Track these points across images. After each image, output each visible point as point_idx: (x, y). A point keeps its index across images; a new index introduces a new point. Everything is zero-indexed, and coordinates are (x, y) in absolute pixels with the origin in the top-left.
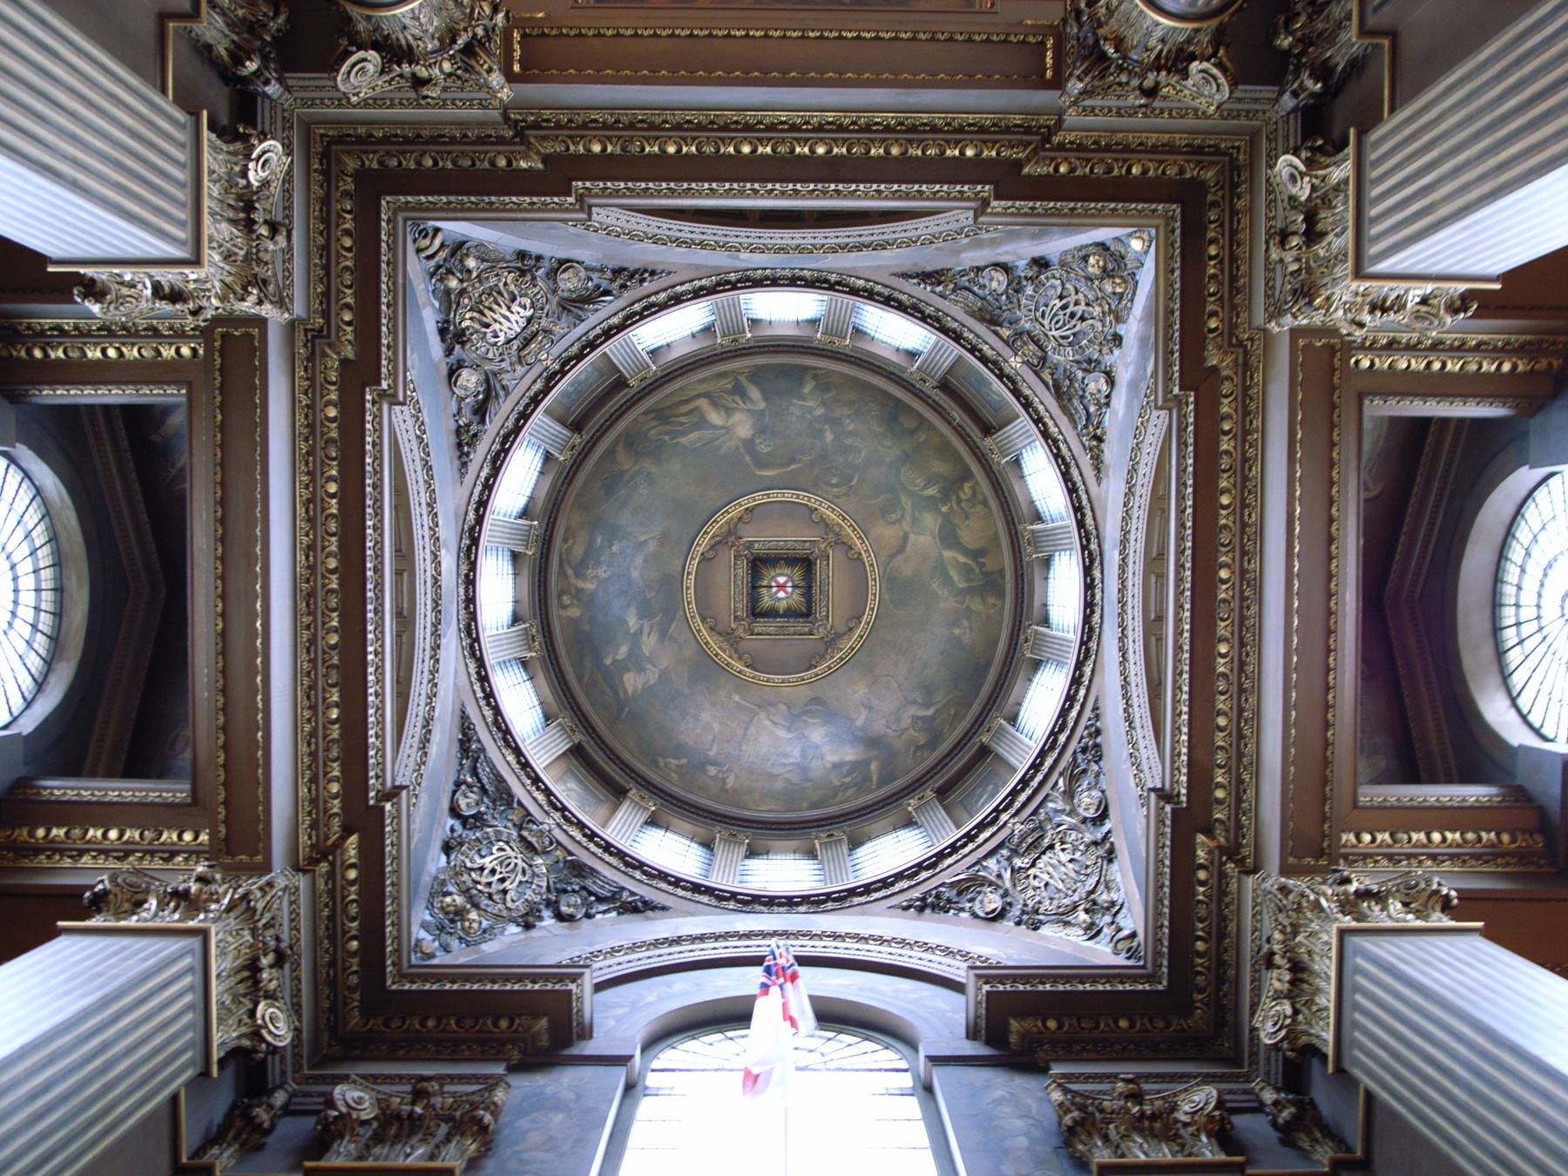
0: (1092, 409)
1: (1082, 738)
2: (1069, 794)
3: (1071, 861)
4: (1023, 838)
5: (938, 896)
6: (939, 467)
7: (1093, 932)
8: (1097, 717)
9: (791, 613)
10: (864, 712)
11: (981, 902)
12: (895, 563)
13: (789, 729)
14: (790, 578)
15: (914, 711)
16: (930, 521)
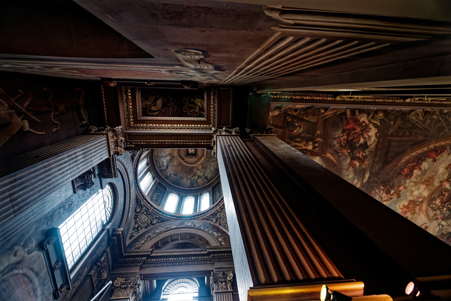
0: (211, 219)
1: (165, 218)
2: (156, 218)
3: (145, 221)
4: (149, 212)
5: (139, 201)
6: (209, 176)
7: (134, 229)
8: (168, 221)
9: (188, 152)
10: (172, 165)
11: (138, 208)
12: (195, 168)
13: (169, 154)
14: (193, 152)
15: (172, 172)
16: (202, 174)
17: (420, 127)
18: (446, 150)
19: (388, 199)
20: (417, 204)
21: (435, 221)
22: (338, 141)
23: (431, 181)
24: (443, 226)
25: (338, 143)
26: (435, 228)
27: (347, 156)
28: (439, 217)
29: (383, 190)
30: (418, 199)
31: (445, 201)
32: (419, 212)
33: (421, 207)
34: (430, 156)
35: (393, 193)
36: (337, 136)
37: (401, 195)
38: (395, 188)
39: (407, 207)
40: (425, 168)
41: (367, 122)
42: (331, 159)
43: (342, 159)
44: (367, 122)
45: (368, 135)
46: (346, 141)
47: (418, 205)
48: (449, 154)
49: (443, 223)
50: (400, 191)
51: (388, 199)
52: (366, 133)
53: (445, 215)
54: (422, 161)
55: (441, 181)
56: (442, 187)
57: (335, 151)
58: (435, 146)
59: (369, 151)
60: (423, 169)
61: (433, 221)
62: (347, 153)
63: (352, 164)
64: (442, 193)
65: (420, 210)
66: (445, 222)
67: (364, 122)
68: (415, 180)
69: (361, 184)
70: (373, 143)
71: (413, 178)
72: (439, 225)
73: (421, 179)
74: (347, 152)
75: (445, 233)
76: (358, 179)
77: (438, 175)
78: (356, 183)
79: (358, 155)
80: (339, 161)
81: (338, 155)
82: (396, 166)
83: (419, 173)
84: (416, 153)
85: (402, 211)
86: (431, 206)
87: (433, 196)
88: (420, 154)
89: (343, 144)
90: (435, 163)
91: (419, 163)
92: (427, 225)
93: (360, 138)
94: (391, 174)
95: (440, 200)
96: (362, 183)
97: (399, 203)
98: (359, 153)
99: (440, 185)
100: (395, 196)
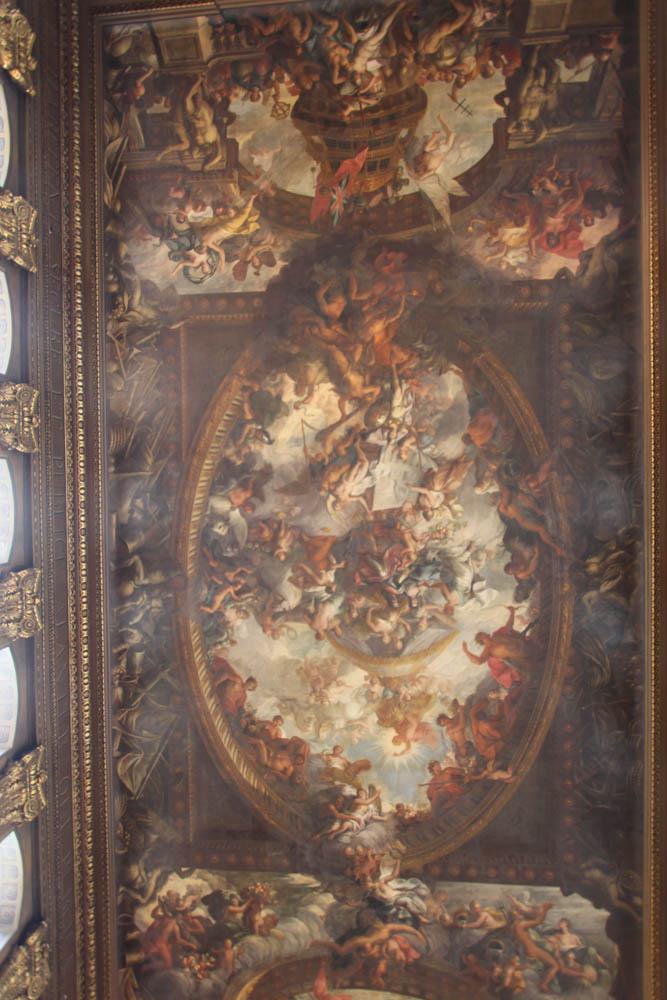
17: (160, 754)
18: (222, 656)
19: (373, 798)
20: (394, 697)
21: (455, 616)
22: (203, 975)
23: (314, 673)
24: (476, 579)
25: (209, 977)
26: (482, 603)
27: (243, 945)
28: (441, 602)
29: (343, 821)
30: (375, 697)
31: (385, 601)
32: (420, 683)
33: (401, 679)
34: (238, 701)
35: (354, 786)
36: (192, 981)
37: (362, 758)
38: (337, 783)
39: (401, 727)
40: (274, 705)
41: (153, 905)
42: (252, 989)
43: (250, 960)
44: (153, 905)
45: (185, 897)
46: (203, 956)
47: (397, 693)
48: (233, 643)
49: (464, 581)
50: (348, 765)
51: (373, 798)
52: (181, 903)
53: (434, 586)
54: (253, 722)
55: (314, 640)
56: (334, 630)
57: (228, 982)
58: (211, 696)
59: (228, 888)
60: (277, 712)
61: (454, 621)
62: (235, 948)
63: (264, 930)
64: (355, 622)
65: (412, 679)
66: (462, 575)
67: (154, 914)
68: (311, 728)
69: (326, 891)
70: (205, 880)
71: (307, 733)
72: (471, 594)
73: (307, 709)
74: (233, 946)
75: (507, 558)
76: (311, 902)
77: (295, 657)
78: (323, 908)
79: (240, 916)
80: (257, 969)
81: (240, 971)
82: (269, 798)
83: (289, 719)
84: (231, 748)
85: (416, 740)
86: (399, 645)
87: (365, 648)
88: (232, 736)
89: (211, 963)
90: (259, 678)
91: (259, 731)
92: (470, 637)
93: (193, 918)
94: (294, 811)
95: (381, 621)
96: (321, 890)
97: (389, 759)
98: (233, 913)
99: (330, 637)
100: (367, 778)
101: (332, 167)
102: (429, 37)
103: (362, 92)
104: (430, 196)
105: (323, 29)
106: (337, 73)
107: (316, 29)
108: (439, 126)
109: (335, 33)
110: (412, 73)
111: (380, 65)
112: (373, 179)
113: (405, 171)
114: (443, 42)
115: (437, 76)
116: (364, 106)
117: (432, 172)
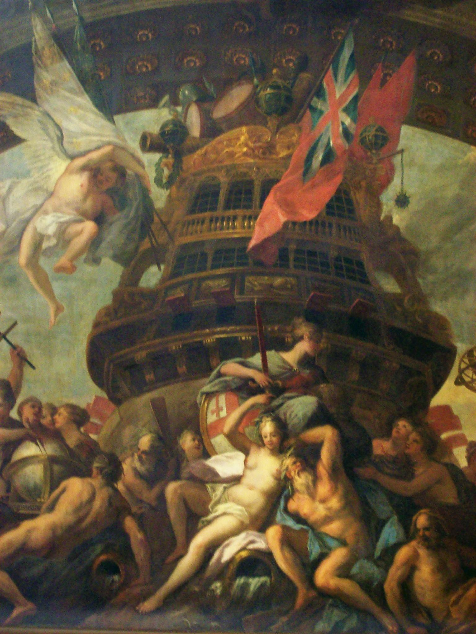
101: (349, 202)
102: (80, 520)
103: (259, 399)
104: (85, 101)
105: (355, 570)
106: (325, 454)
107: (372, 570)
108: (57, 287)
109: (322, 557)
110: (128, 432)
111: (211, 462)
112: (239, 160)
113: (151, 174)
114: (47, 500)
115: (61, 419)
116: (257, 359)
117: (80, 162)
